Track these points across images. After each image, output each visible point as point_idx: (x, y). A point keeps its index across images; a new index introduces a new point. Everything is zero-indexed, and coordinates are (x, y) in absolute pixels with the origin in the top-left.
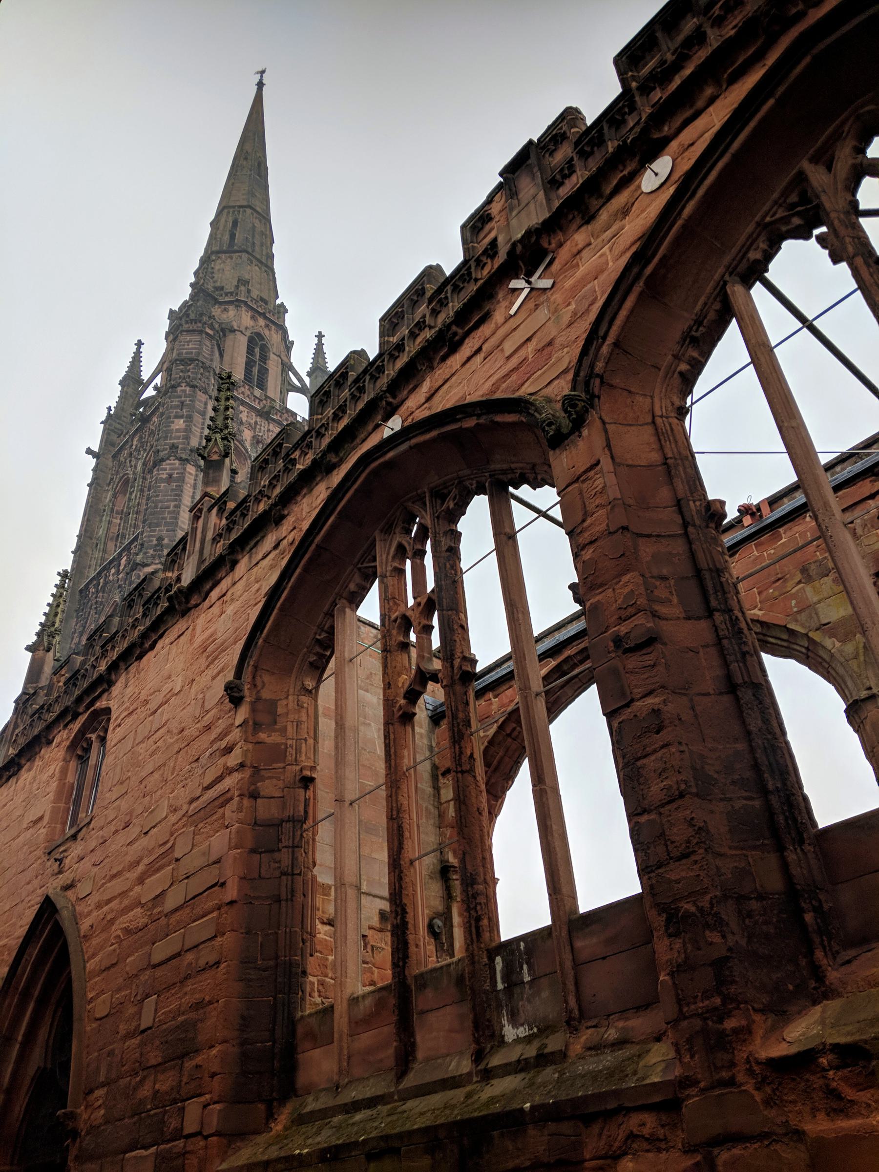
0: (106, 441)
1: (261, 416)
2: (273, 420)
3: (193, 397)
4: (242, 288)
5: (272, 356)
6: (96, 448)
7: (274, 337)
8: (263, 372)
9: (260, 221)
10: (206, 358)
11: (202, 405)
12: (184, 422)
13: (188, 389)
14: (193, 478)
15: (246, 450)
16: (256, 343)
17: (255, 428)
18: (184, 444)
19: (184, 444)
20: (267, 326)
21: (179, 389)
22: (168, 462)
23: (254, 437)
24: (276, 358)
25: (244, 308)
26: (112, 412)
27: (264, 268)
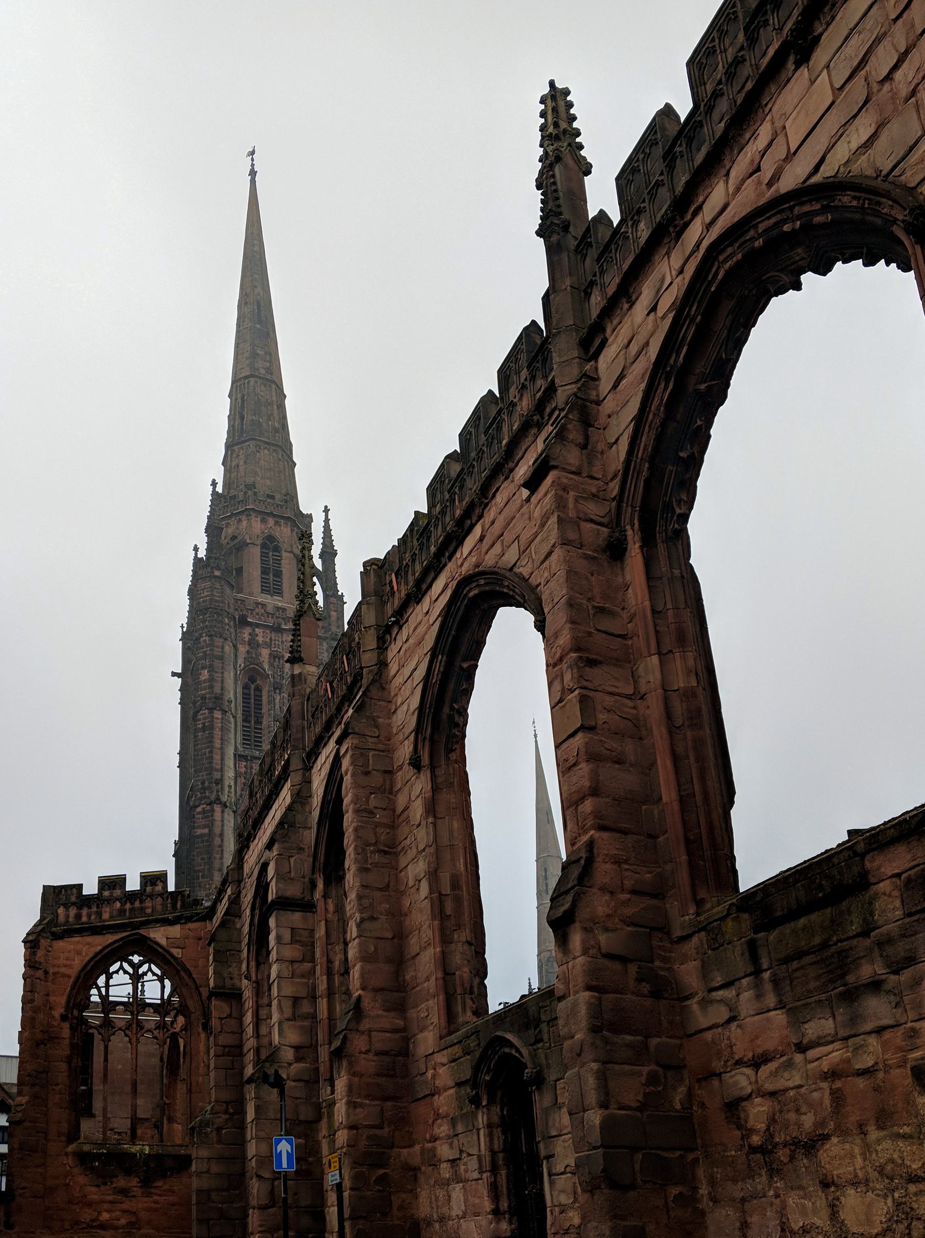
2: (285, 629)
3: (212, 645)
4: (250, 493)
5: (284, 554)
7: (285, 534)
8: (278, 574)
9: (265, 386)
10: (218, 602)
11: (220, 650)
14: (219, 721)
15: (265, 670)
16: (270, 544)
17: (271, 645)
18: (209, 693)
19: (209, 693)
20: (277, 523)
21: (202, 639)
22: (201, 712)
23: (270, 654)
24: (288, 554)
25: (253, 515)
27: (272, 448)
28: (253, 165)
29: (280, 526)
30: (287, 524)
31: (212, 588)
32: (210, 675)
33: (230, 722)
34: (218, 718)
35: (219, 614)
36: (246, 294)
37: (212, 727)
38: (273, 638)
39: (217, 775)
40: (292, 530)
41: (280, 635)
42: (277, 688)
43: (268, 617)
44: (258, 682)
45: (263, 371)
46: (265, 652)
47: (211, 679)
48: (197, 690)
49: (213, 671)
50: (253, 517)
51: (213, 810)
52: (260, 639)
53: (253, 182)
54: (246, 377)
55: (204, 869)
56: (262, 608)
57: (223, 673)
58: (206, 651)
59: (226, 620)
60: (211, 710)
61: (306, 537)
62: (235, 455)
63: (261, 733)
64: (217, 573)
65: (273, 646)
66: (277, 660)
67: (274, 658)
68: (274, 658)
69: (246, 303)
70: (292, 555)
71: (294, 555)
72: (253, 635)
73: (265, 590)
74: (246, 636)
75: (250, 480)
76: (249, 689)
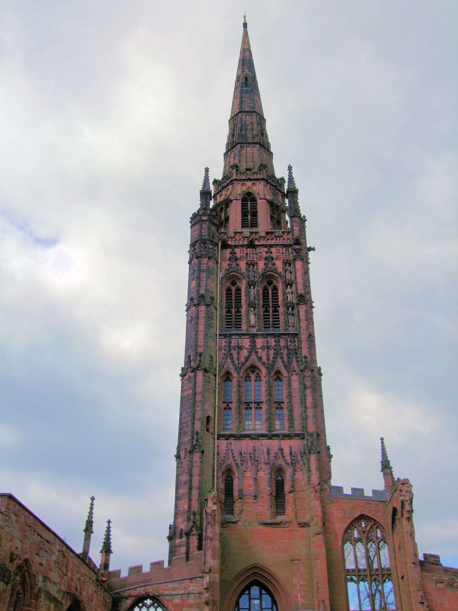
1: (249, 248)
5: (259, 201)
8: (255, 214)
9: (249, 115)
14: (203, 313)
23: (247, 263)
24: (263, 201)
33: (213, 313)
35: (205, 243)
38: (248, 253)
39: (200, 350)
41: (254, 250)
42: (252, 285)
44: (238, 284)
51: (195, 375)
52: (238, 255)
55: (188, 420)
59: (211, 246)
64: (205, 218)
65: (248, 258)
66: (251, 266)
70: (265, 201)
71: (267, 200)
74: (228, 255)
76: (231, 290)
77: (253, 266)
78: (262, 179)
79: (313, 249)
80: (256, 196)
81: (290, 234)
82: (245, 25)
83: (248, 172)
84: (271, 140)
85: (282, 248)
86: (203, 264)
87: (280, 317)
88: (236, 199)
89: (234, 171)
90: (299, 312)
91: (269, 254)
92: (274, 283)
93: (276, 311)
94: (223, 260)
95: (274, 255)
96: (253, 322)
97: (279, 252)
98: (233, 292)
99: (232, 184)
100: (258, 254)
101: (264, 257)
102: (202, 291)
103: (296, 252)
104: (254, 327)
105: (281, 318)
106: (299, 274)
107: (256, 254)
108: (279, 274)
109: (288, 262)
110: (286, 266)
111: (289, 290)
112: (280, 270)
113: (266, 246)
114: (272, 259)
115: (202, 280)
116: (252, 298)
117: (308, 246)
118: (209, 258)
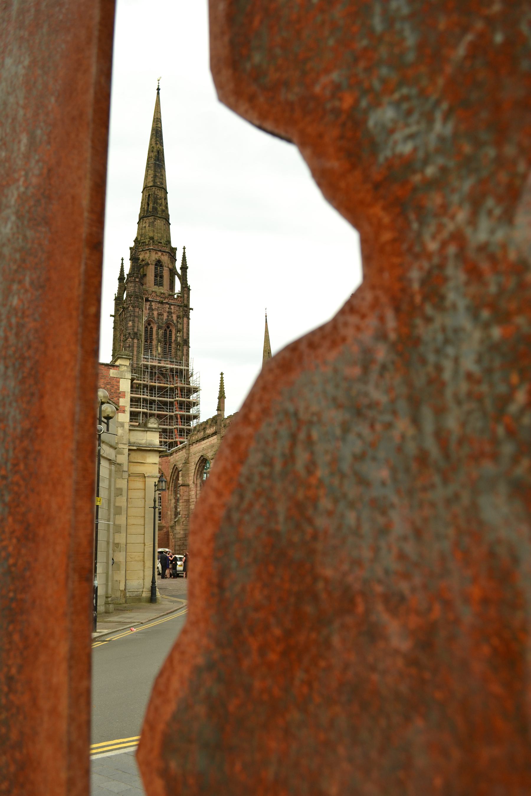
0: (116, 310)
1: (159, 303)
2: (165, 303)
5: (165, 268)
6: (113, 314)
7: (165, 259)
8: (161, 277)
9: (159, 190)
12: (132, 323)
13: (132, 308)
14: (136, 344)
21: (129, 308)
22: (128, 339)
23: (158, 314)
26: (116, 296)
27: (161, 219)
28: (159, 86)
29: (163, 255)
30: (167, 255)
31: (135, 286)
32: (133, 324)
34: (135, 343)
35: (137, 298)
36: (153, 147)
37: (133, 347)
40: (169, 257)
41: (162, 305)
43: (157, 297)
45: (159, 183)
46: (155, 313)
47: (133, 326)
48: (127, 330)
49: (134, 323)
50: (152, 252)
52: (154, 307)
53: (158, 93)
54: (151, 186)
56: (155, 293)
57: (138, 323)
58: (131, 314)
59: (140, 300)
60: (133, 339)
61: (173, 259)
62: (144, 222)
63: (152, 347)
65: (159, 310)
66: (160, 316)
67: (159, 315)
68: (159, 315)
69: (152, 151)
70: (168, 269)
71: (169, 268)
72: (151, 305)
73: (156, 284)
75: (151, 234)
76: (148, 328)
77: (161, 315)
78: (168, 252)
79: (192, 309)
80: (163, 264)
81: (182, 298)
82: (158, 89)
83: (159, 244)
84: (170, 212)
85: (177, 307)
86: (136, 312)
87: (172, 349)
88: (152, 264)
89: (151, 241)
90: (183, 350)
91: (170, 310)
92: (171, 328)
93: (170, 345)
94: (146, 309)
95: (172, 311)
96: (159, 351)
97: (175, 309)
98: (149, 329)
99: (149, 251)
100: (164, 309)
101: (167, 311)
102: (136, 330)
103: (185, 312)
104: (160, 354)
105: (173, 351)
106: (185, 326)
107: (163, 308)
108: (174, 324)
109: (179, 317)
110: (178, 319)
111: (178, 335)
112: (175, 322)
113: (169, 304)
114: (172, 313)
115: (136, 323)
116: (160, 336)
117: (190, 307)
118: (140, 309)
